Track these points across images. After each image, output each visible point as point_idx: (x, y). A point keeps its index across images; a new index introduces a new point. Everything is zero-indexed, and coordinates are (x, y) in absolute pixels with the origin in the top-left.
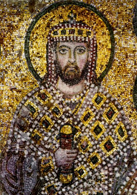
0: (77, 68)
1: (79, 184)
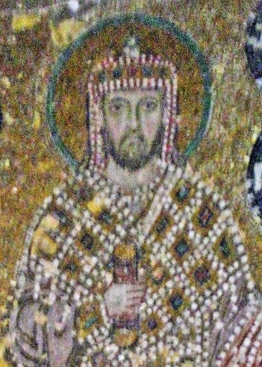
0: (142, 138)
1: (150, 346)
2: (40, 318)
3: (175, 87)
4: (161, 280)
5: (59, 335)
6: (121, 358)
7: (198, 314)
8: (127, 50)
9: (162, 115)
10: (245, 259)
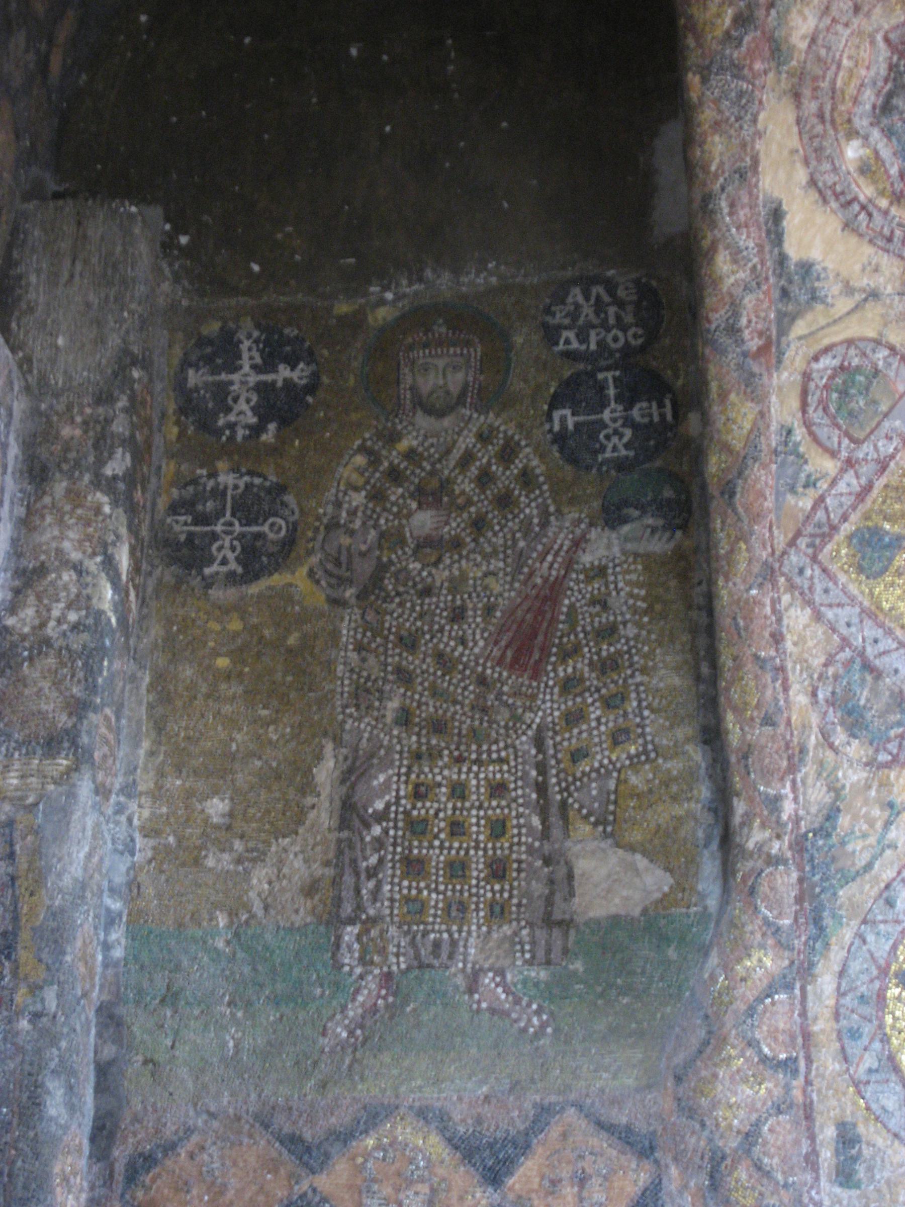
0: (448, 393)
1: (453, 562)
2: (346, 541)
3: (479, 354)
4: (465, 506)
5: (363, 555)
6: (425, 574)
7: (501, 534)
8: (435, 328)
9: (467, 375)
10: (545, 487)
